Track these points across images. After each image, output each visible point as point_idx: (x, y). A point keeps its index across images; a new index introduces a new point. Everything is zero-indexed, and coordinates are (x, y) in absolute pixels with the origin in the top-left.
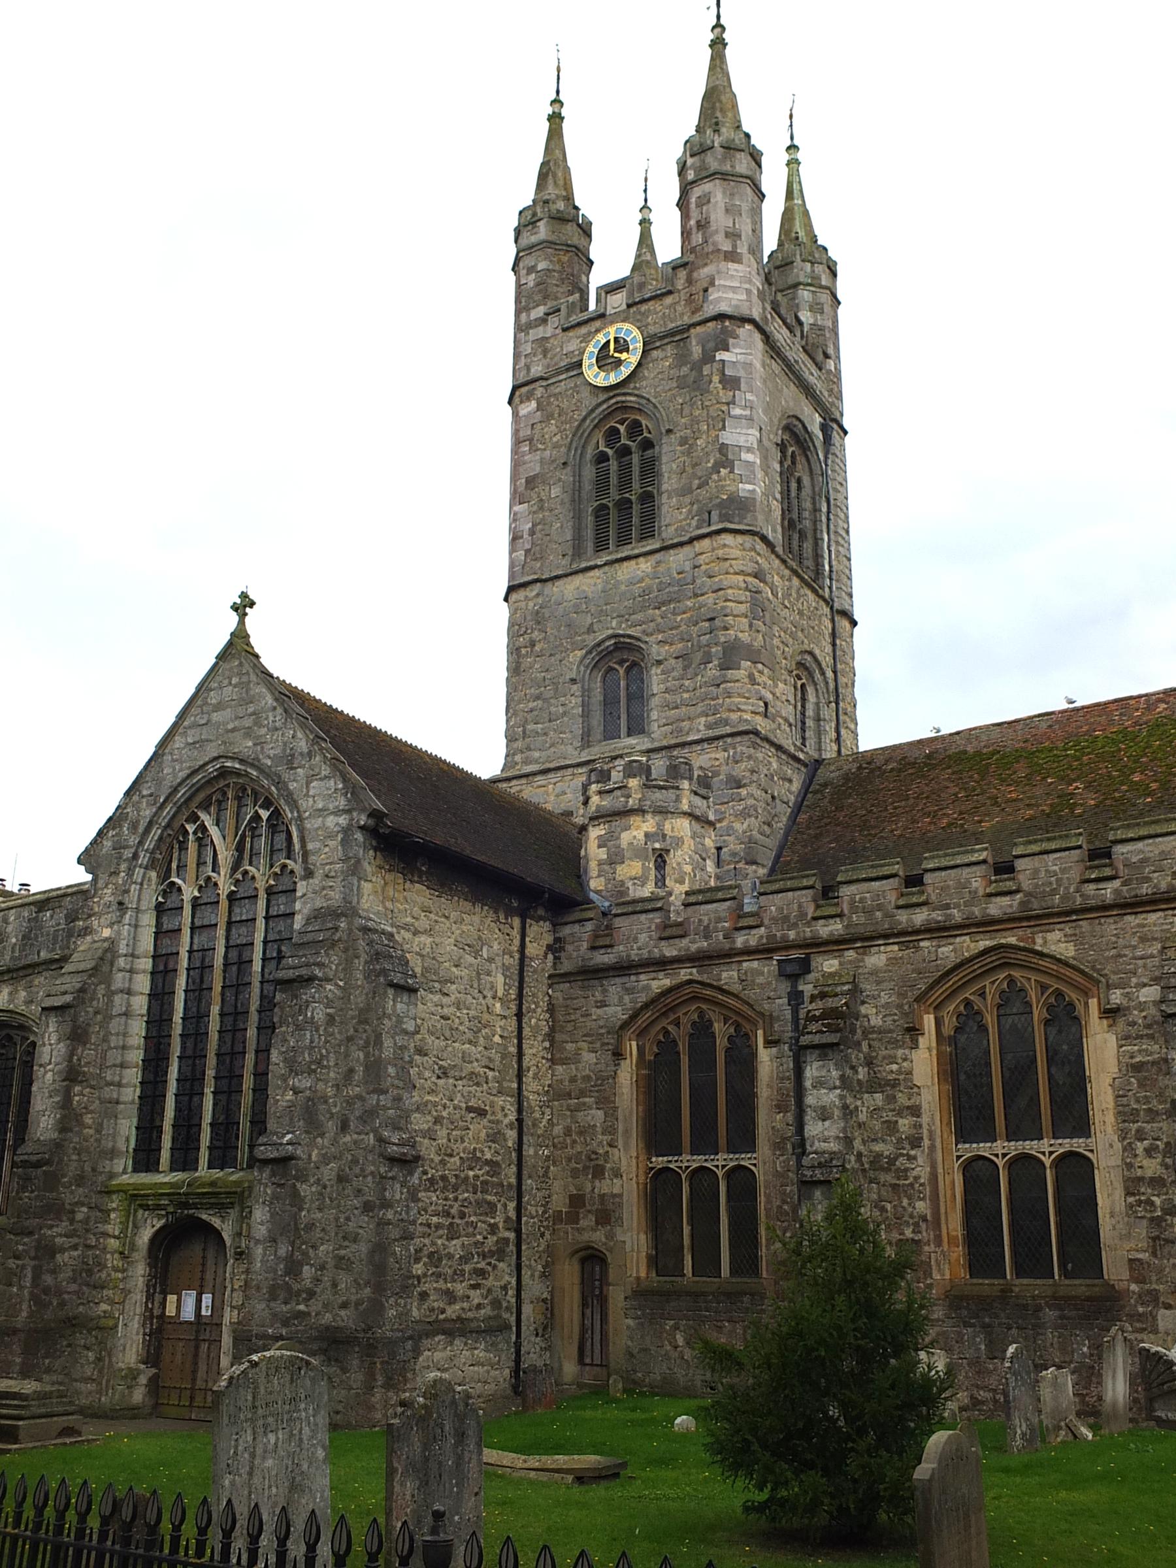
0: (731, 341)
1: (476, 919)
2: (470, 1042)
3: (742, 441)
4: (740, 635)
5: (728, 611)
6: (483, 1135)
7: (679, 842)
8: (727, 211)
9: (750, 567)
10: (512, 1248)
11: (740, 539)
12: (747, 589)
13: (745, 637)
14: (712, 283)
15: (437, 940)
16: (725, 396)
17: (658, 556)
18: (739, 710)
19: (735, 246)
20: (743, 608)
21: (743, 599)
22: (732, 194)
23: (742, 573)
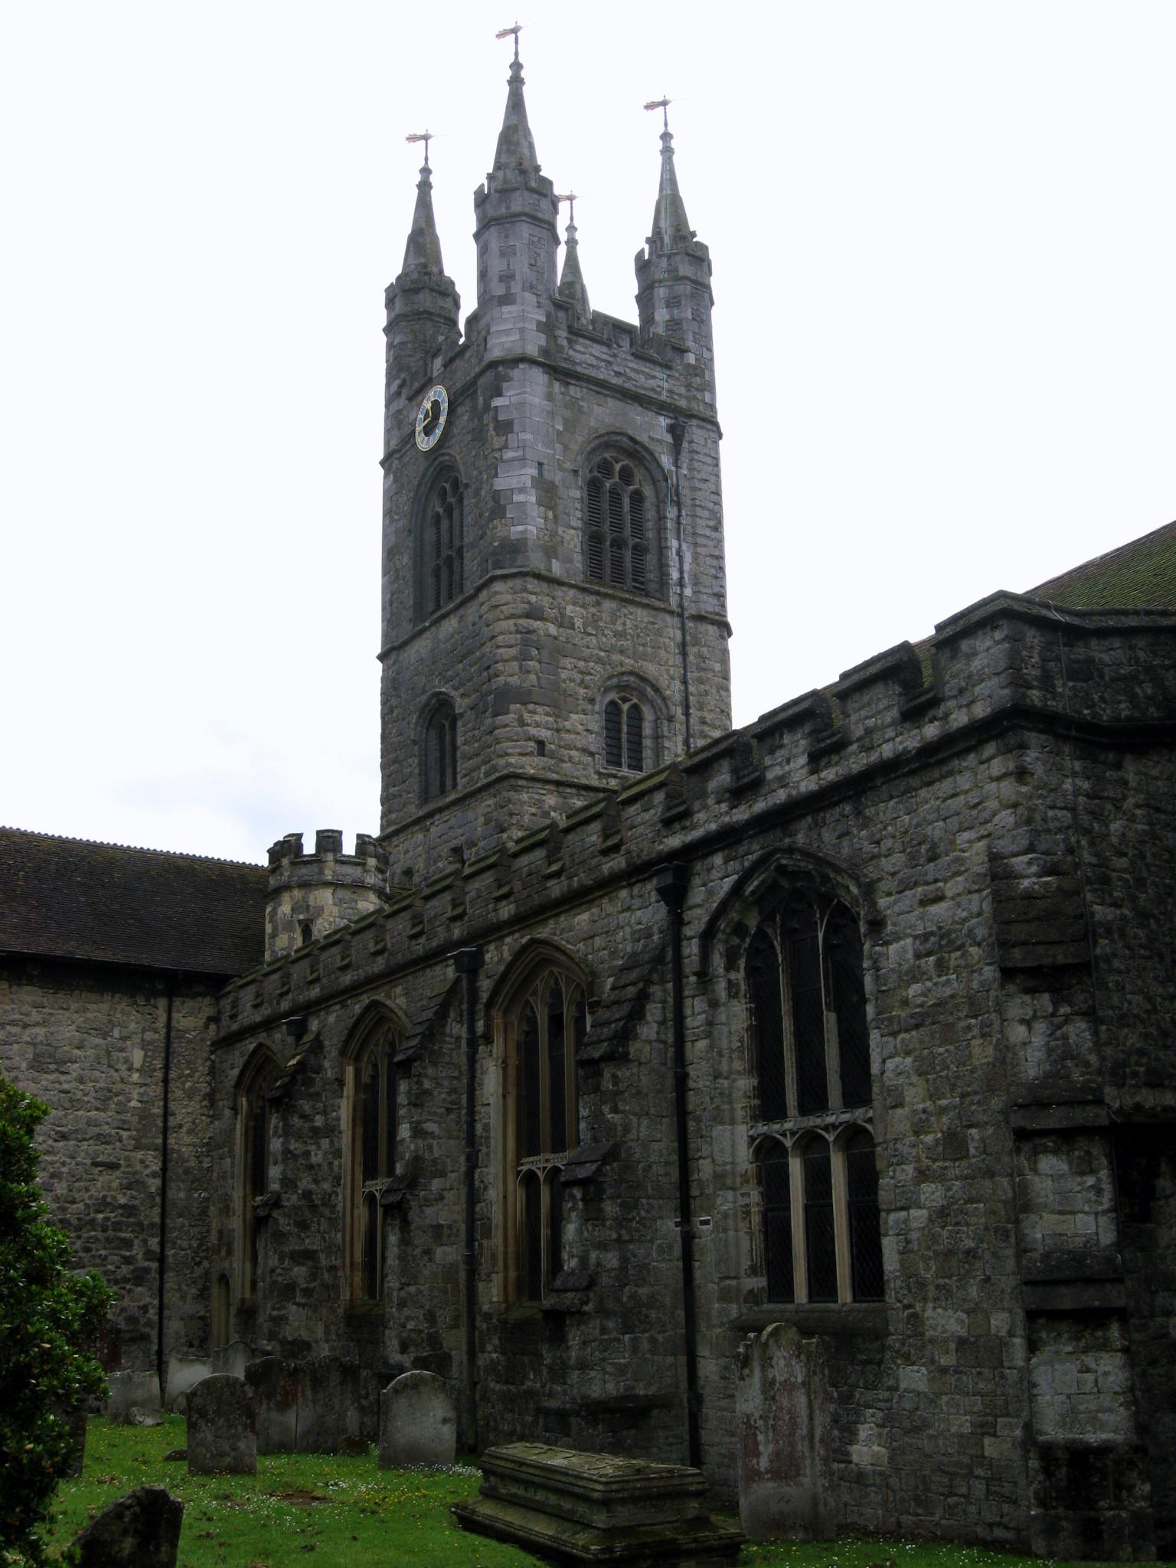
0: (505, 385)
1: (105, 1007)
2: (97, 1109)
3: (514, 483)
4: (510, 679)
5: (498, 657)
6: (115, 1185)
7: (320, 910)
8: (502, 254)
9: (522, 607)
10: (154, 1274)
11: (510, 583)
12: (518, 632)
13: (514, 681)
14: (488, 332)
15: (53, 1029)
16: (497, 442)
17: (461, 612)
18: (507, 754)
19: (509, 288)
20: (513, 652)
21: (513, 642)
22: (506, 237)
23: (512, 616)
